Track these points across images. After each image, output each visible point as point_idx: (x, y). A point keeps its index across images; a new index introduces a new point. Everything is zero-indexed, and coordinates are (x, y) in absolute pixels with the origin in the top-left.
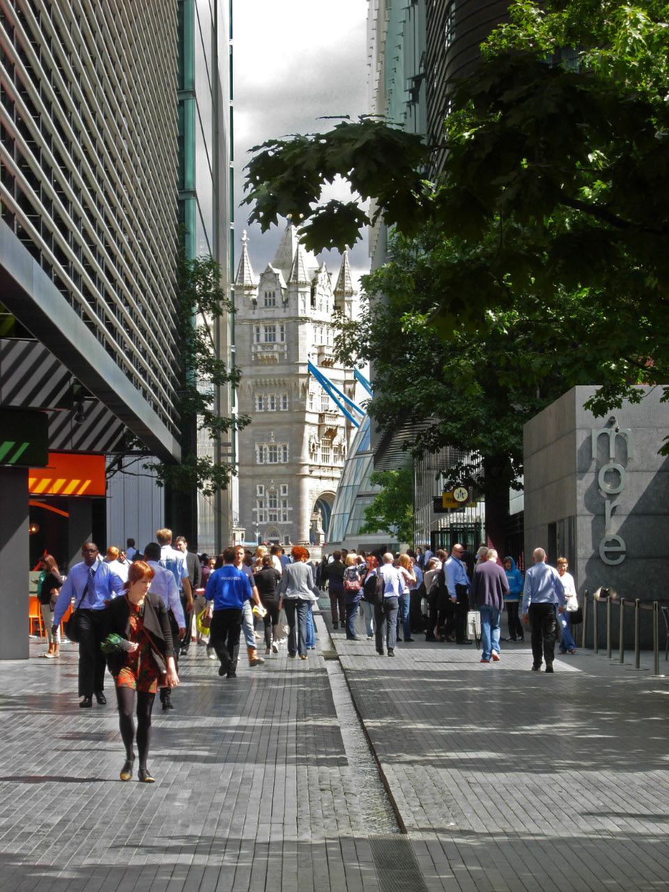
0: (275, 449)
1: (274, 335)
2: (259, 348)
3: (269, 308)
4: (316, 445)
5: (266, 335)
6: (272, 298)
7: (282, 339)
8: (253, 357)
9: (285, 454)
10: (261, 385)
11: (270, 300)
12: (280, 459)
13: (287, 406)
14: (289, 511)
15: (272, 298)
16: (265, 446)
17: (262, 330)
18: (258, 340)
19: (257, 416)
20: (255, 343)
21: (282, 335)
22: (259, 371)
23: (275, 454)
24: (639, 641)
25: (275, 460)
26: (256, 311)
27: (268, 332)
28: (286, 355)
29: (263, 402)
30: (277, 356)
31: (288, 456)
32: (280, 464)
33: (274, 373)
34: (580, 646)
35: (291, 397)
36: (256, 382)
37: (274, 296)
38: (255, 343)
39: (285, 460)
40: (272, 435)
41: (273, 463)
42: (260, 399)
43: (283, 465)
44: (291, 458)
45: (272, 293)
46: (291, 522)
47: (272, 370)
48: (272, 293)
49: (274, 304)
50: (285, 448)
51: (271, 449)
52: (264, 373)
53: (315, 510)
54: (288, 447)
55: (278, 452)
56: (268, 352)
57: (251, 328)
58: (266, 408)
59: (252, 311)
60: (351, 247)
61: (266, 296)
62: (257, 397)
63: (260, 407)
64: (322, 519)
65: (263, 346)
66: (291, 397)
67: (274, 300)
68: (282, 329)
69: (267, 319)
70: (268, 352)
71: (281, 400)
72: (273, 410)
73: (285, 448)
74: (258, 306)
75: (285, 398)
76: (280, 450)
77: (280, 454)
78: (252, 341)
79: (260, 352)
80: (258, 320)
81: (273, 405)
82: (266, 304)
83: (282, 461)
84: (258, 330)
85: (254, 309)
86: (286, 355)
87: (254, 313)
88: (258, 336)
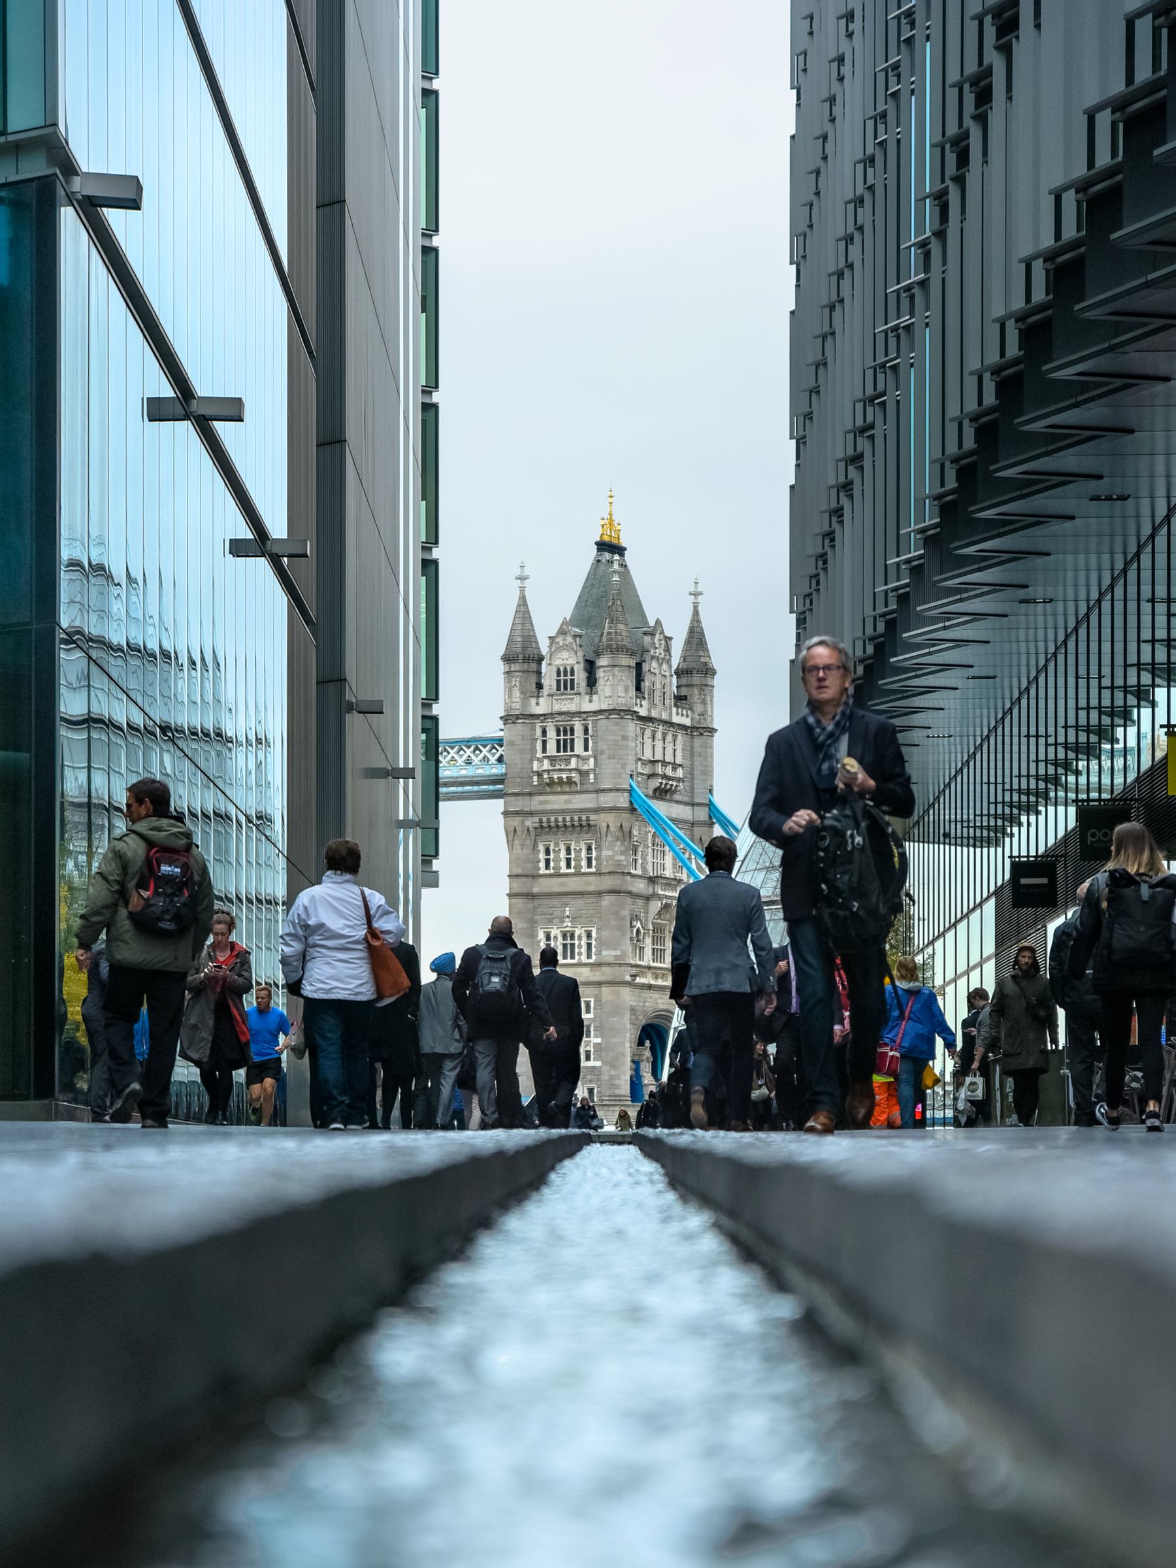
0: (572, 937)
1: (572, 740)
2: (546, 765)
3: (563, 694)
4: (642, 931)
5: (558, 741)
6: (569, 677)
7: (586, 749)
8: (535, 779)
9: (589, 946)
10: (573, 825)
11: (565, 681)
12: (580, 954)
13: (594, 863)
14: (596, 1045)
15: (569, 677)
16: (555, 932)
17: (551, 734)
18: (544, 750)
19: (541, 880)
20: (539, 754)
21: (586, 740)
22: (546, 802)
23: (573, 945)
24: (61, 1081)
25: (572, 957)
26: (541, 700)
27: (562, 737)
28: (592, 776)
29: (552, 856)
30: (575, 776)
31: (594, 950)
32: (580, 965)
33: (571, 806)
34: (176, 1116)
35: (598, 848)
36: (541, 821)
37: (572, 673)
38: (539, 754)
39: (589, 956)
40: (567, 913)
41: (569, 961)
42: (547, 852)
43: (585, 965)
44: (599, 953)
45: (569, 669)
46: (598, 1064)
47: (567, 802)
48: (569, 669)
49: (572, 688)
50: (589, 936)
51: (564, 937)
52: (557, 807)
53: (641, 1043)
54: (594, 934)
55: (577, 942)
56: (560, 770)
57: (534, 729)
58: (557, 868)
59: (533, 701)
60: (565, 618)
61: (559, 674)
62: (541, 848)
63: (547, 866)
64: (651, 1059)
65: (552, 759)
66: (598, 848)
67: (572, 681)
68: (586, 730)
69: (561, 714)
70: (560, 770)
71: (584, 854)
72: (548, 872)
73: (589, 936)
74: (546, 691)
75: (589, 849)
76: (580, 938)
77: (580, 947)
78: (534, 750)
79: (548, 771)
80: (544, 717)
81: (568, 861)
82: (558, 689)
83: (584, 959)
84: (544, 732)
85: (538, 697)
86: (592, 776)
87: (537, 704)
88: (544, 743)
